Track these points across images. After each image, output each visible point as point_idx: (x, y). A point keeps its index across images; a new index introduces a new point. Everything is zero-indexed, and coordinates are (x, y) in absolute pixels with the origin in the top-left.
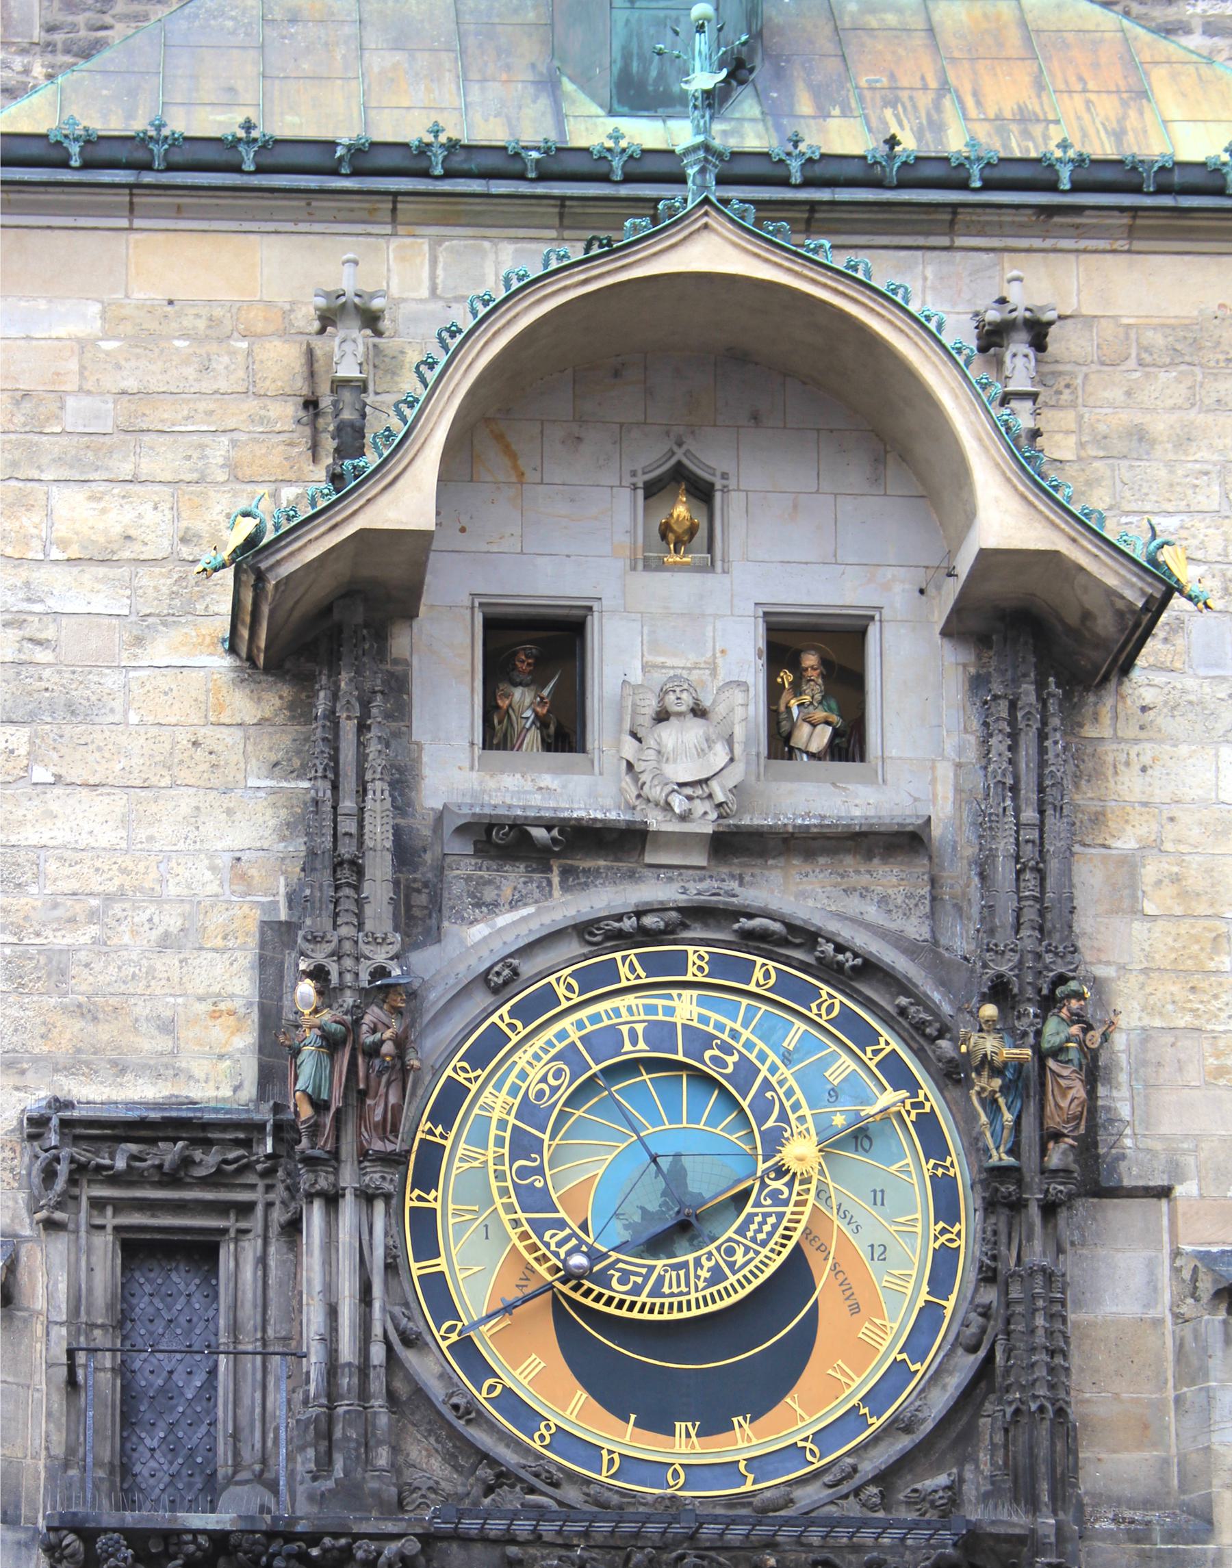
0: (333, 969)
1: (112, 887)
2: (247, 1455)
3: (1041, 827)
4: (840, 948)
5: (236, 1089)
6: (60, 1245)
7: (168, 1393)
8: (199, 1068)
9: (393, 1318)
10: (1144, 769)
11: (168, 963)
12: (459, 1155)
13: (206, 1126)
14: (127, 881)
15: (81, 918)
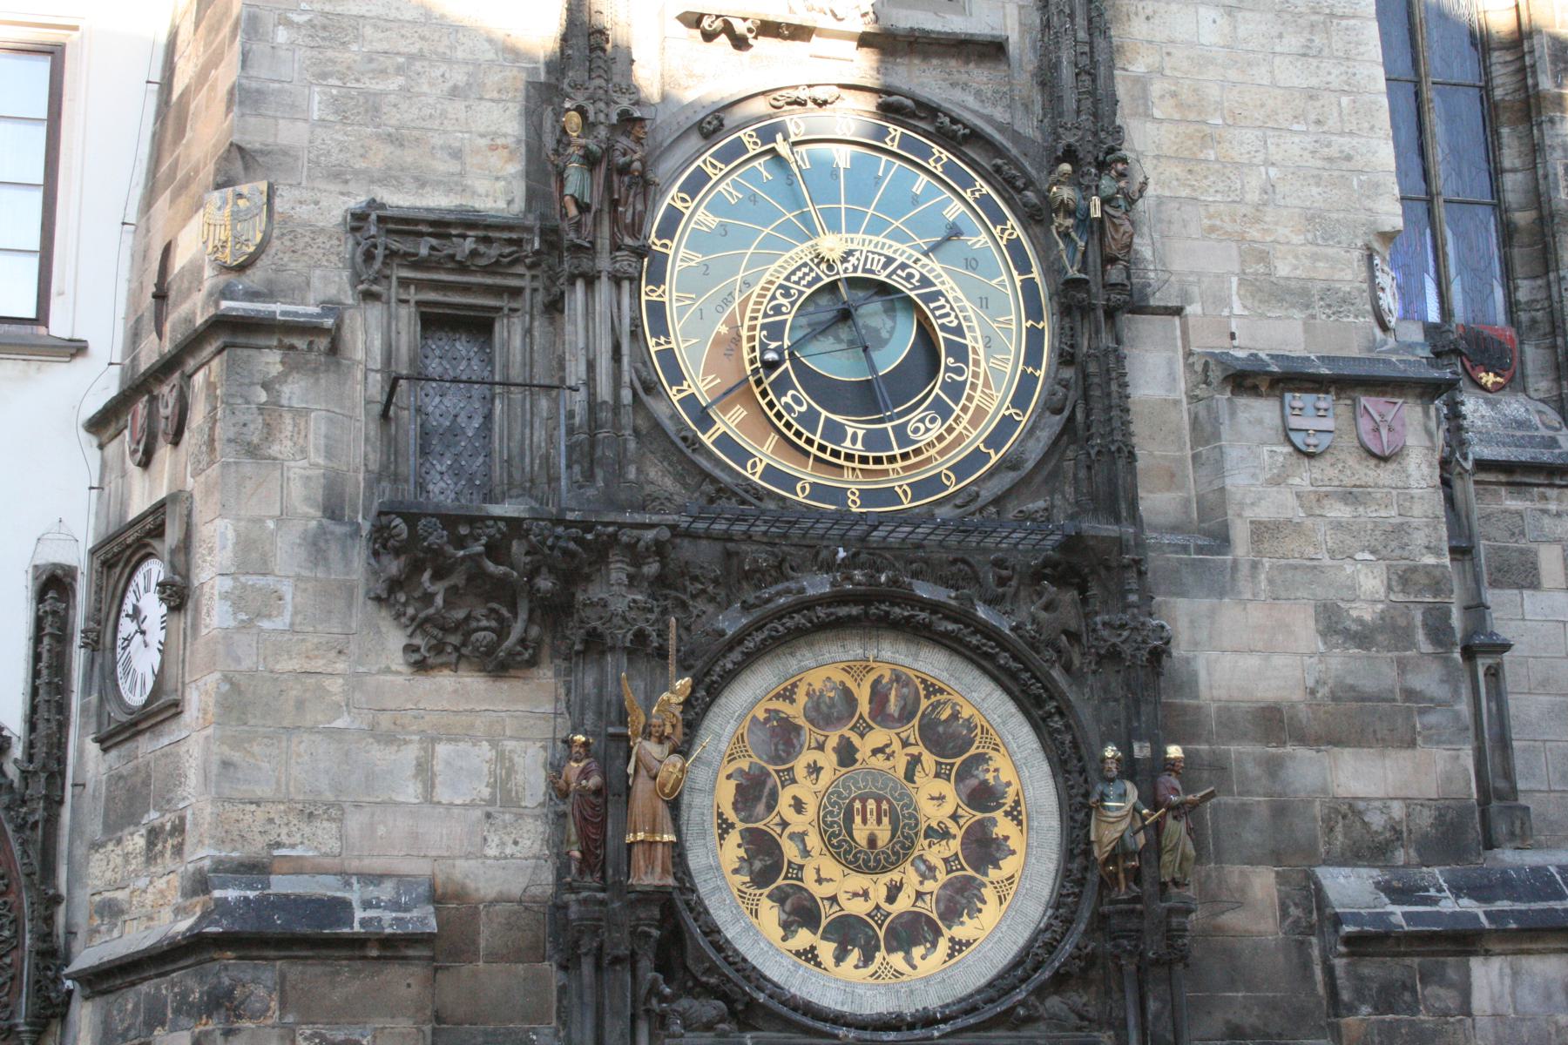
0: (591, 110)
1: (414, 50)
2: (517, 475)
3: (1091, 44)
4: (954, 121)
5: (509, 203)
6: (375, 312)
7: (454, 431)
8: (481, 185)
9: (637, 371)
10: (1148, 18)
11: (457, 108)
12: (680, 255)
13: (488, 227)
14: (425, 46)
15: (391, 70)
